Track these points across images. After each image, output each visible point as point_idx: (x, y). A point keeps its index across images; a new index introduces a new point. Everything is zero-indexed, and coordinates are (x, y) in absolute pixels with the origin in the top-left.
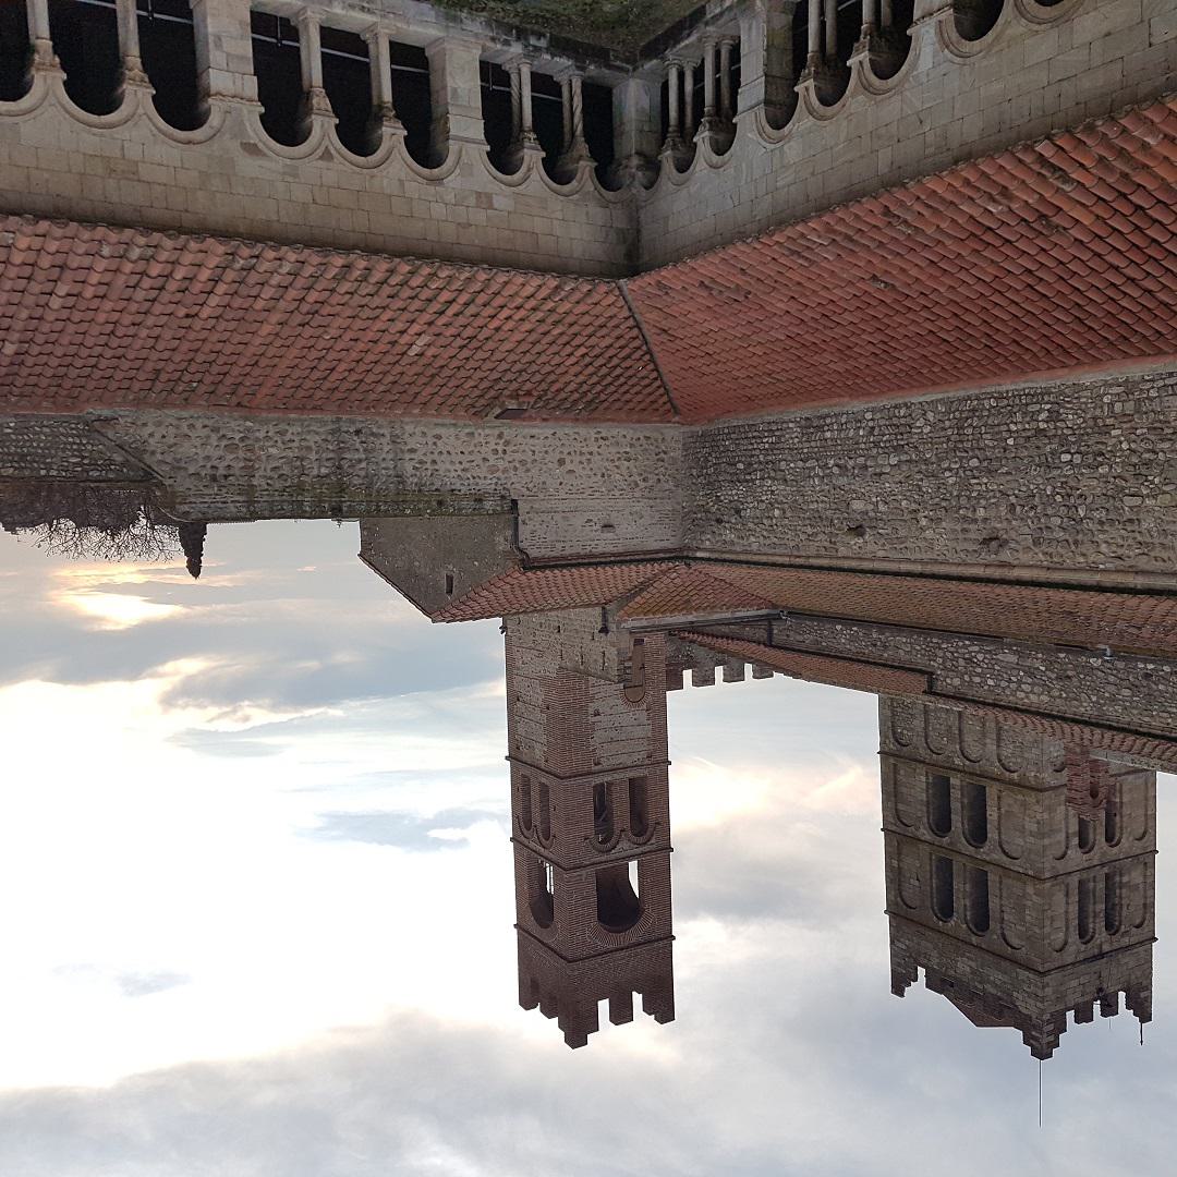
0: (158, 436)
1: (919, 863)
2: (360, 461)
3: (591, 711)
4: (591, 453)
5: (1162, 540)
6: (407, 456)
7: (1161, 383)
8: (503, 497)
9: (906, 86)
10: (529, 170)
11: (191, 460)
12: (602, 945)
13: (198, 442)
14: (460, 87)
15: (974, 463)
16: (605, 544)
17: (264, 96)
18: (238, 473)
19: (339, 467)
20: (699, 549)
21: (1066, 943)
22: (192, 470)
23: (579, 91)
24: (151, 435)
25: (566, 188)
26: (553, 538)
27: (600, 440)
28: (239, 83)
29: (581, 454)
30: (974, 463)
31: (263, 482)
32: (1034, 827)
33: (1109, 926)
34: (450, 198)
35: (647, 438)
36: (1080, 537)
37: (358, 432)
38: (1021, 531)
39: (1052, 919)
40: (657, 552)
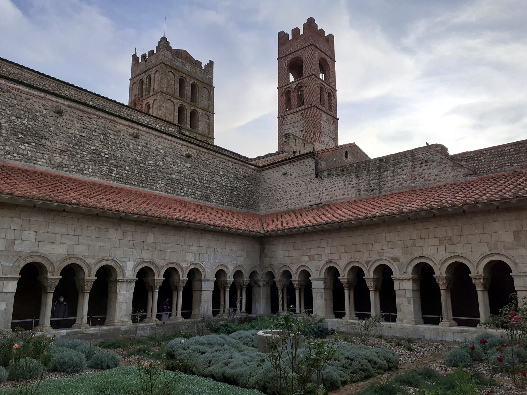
0: (448, 173)
1: (202, 102)
2: (372, 180)
3: (304, 131)
4: (290, 199)
5: (73, 119)
6: (354, 185)
7: (70, 169)
8: (321, 177)
9: (139, 260)
10: (296, 273)
11: (435, 167)
12: (301, 52)
13: (433, 174)
14: (320, 302)
15: (142, 165)
16: (286, 168)
17: (391, 282)
19: (379, 176)
20: (254, 170)
21: (155, 74)
22: (435, 163)
23: (280, 306)
24: (450, 173)
25: (284, 269)
26: (303, 167)
27: (286, 204)
28: (401, 286)
29: (293, 199)
30: (142, 165)
31: (408, 164)
32: (162, 109)
33: (143, 82)
34: (323, 257)
35: (271, 208)
36: (103, 129)
37: (372, 190)
38: (125, 137)
39: (158, 80)
40: (269, 169)
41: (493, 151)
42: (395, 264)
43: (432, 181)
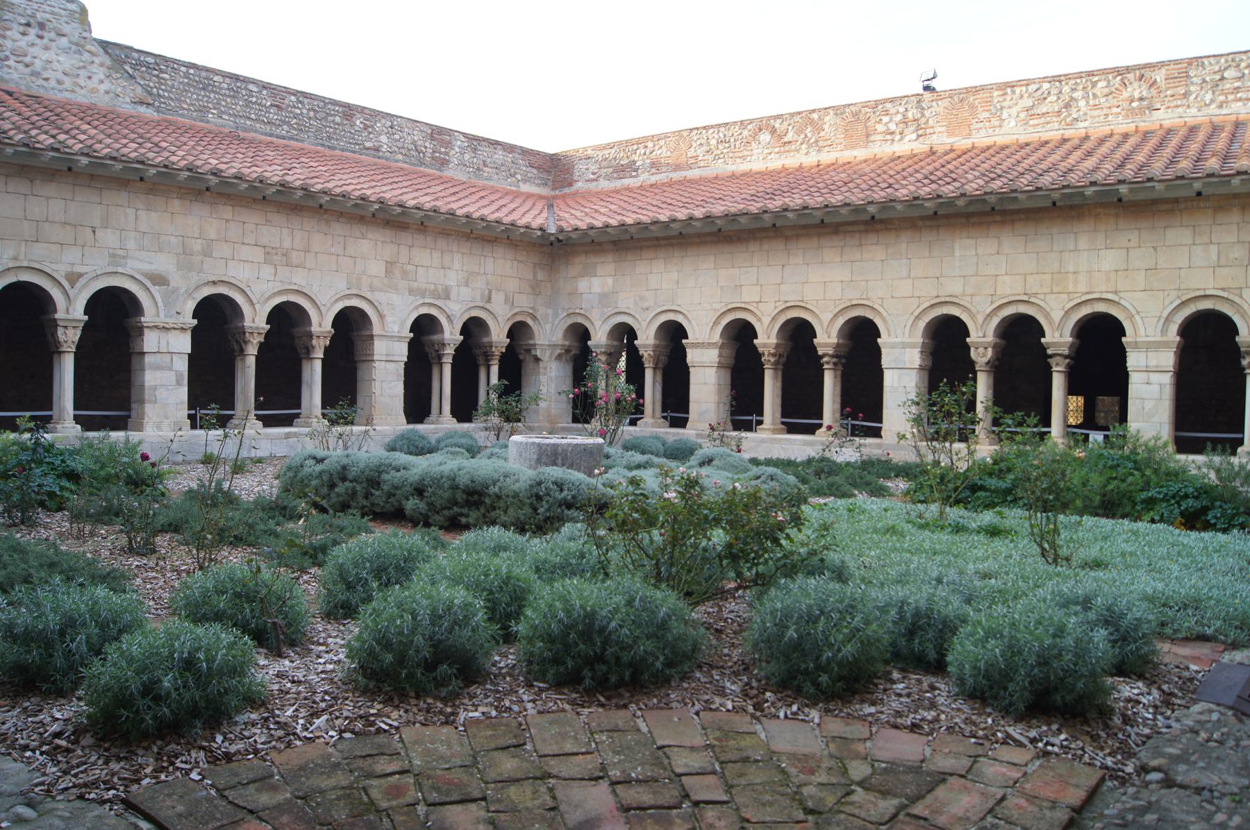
0: (95, 79)
11: (66, 51)
13: (55, 65)
18: (15, 26)
24: (102, 82)
28: (163, 343)
41: (192, 71)
42: (154, 289)
43: (53, 83)
